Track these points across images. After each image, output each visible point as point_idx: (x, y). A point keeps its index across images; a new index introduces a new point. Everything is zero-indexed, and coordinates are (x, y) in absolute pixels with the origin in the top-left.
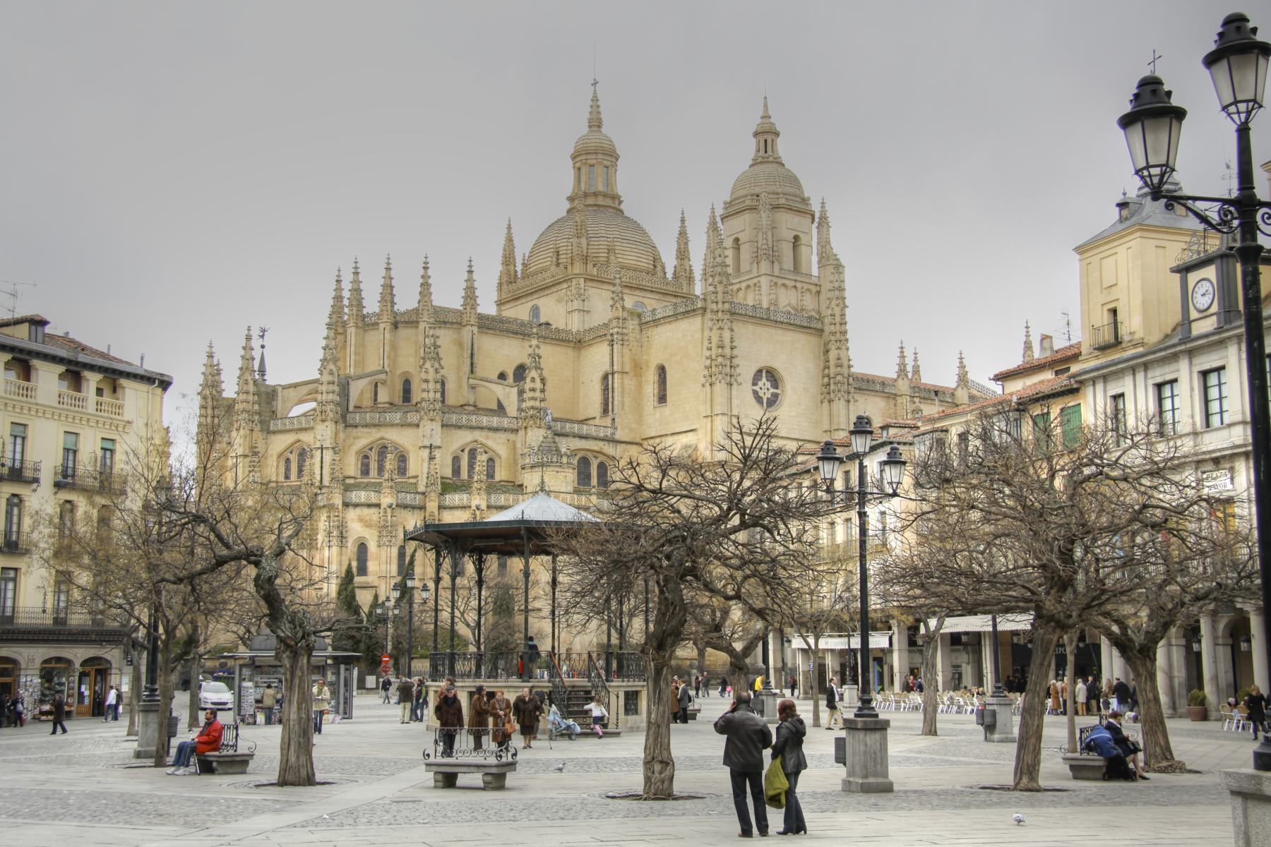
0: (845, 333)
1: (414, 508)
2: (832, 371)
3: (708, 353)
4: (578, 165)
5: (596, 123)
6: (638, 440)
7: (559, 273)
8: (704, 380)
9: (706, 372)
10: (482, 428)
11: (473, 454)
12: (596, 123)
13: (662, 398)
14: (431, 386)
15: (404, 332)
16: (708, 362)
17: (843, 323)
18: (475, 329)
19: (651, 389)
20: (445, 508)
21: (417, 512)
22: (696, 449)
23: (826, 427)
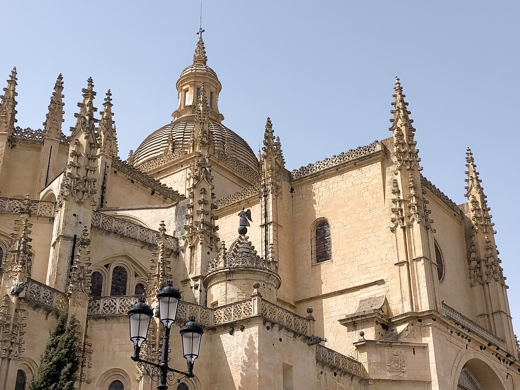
0: (488, 218)
1: (48, 311)
2: (482, 253)
3: (395, 197)
4: (184, 88)
5: (201, 59)
6: (292, 303)
7: (177, 156)
8: (393, 225)
9: (394, 216)
10: (135, 240)
11: (120, 274)
12: (201, 59)
13: (323, 254)
14: (83, 161)
15: (23, 152)
16: (396, 206)
17: (486, 210)
18: (109, 162)
19: (308, 247)
20: (98, 318)
21: (51, 318)
22: (386, 302)
23: (480, 312)
